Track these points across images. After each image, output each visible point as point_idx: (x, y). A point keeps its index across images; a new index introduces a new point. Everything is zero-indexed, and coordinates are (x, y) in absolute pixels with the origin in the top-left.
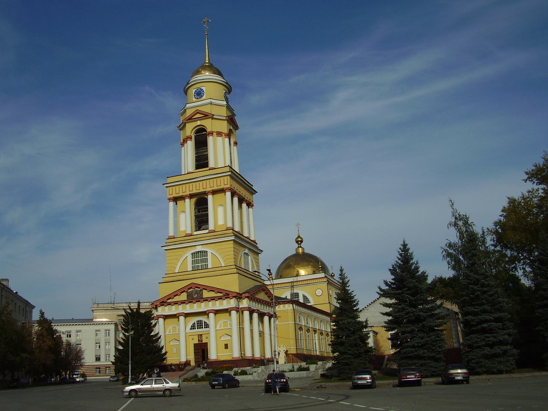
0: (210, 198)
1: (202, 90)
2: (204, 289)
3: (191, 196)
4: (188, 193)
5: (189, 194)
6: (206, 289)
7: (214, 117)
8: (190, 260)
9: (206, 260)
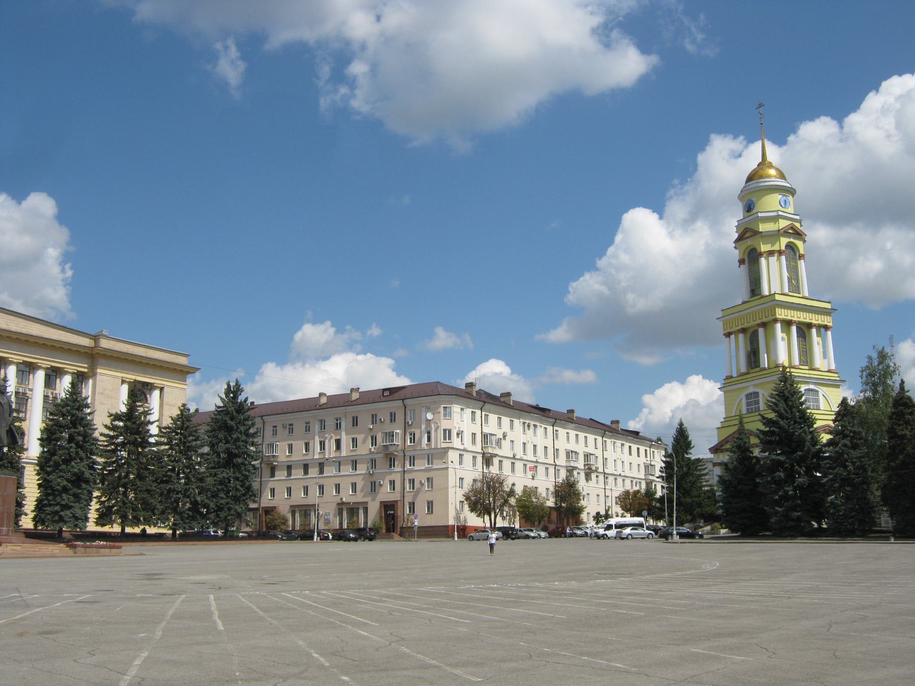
0: (761, 331)
1: (752, 201)
2: (750, 435)
3: (743, 331)
4: (739, 327)
5: (742, 328)
6: (752, 435)
7: (763, 234)
8: (744, 401)
9: (757, 402)
